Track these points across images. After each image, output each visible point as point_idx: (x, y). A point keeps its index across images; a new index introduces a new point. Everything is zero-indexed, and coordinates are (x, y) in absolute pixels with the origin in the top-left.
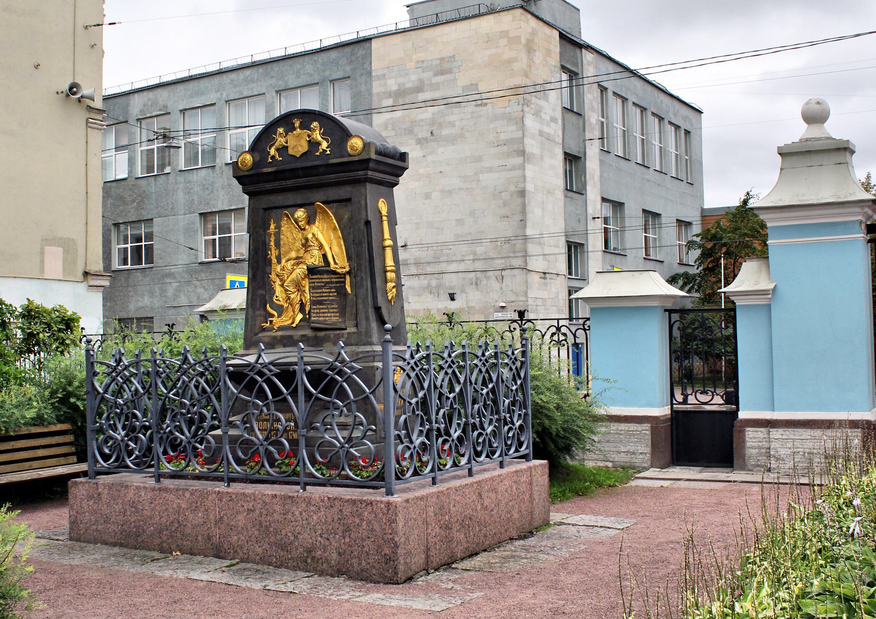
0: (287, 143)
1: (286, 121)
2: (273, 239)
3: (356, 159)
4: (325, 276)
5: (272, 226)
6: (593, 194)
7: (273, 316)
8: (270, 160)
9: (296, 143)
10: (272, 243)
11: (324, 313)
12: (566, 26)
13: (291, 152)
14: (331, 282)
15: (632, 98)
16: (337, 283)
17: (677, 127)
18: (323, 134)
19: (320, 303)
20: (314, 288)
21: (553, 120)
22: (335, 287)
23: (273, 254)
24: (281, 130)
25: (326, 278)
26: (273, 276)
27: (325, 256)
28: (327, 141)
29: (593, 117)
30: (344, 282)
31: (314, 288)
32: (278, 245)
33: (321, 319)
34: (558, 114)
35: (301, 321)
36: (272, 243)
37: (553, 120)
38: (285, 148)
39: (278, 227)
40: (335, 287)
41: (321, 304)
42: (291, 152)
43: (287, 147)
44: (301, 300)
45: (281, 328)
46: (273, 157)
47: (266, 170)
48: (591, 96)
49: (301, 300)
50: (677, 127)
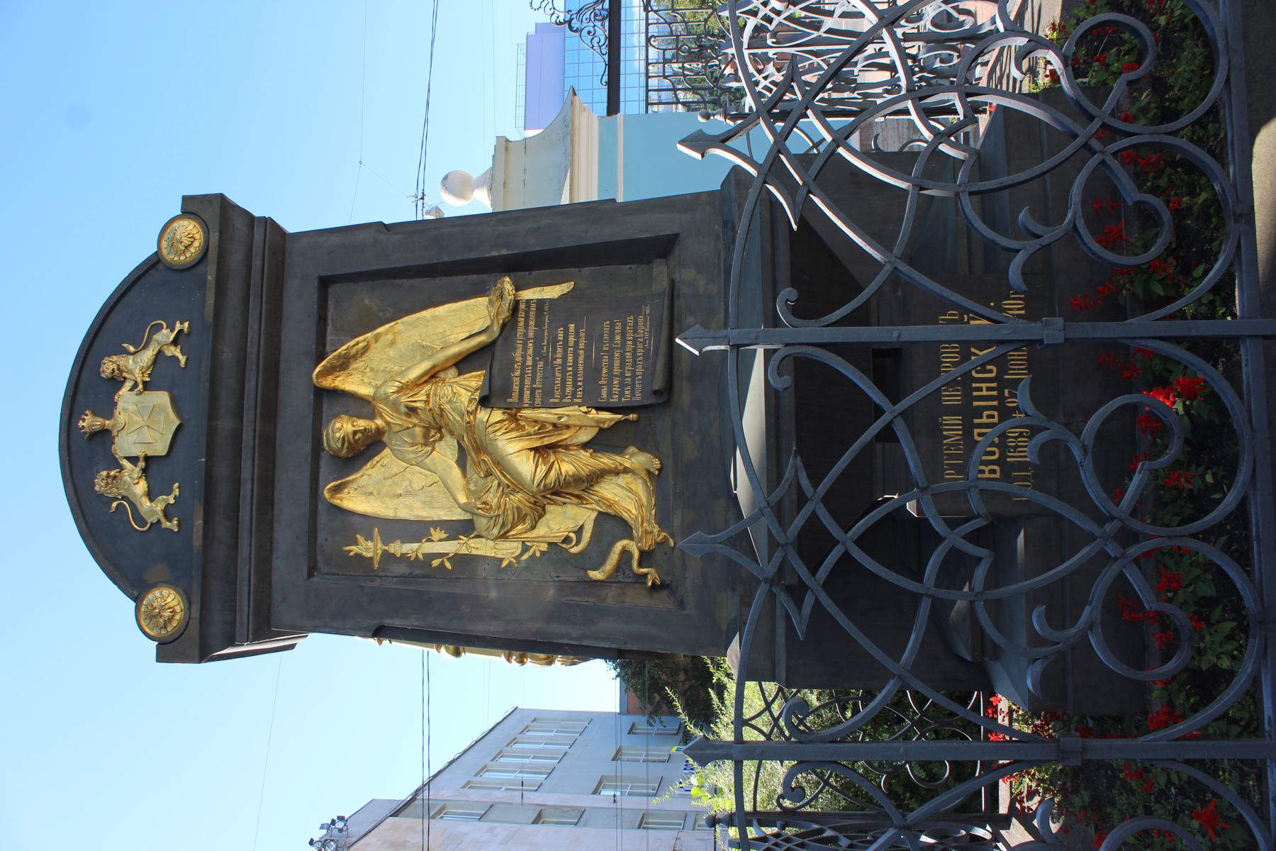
0: (133, 460)
1: (83, 454)
2: (399, 548)
3: (215, 237)
4: (518, 355)
5: (368, 548)
6: (587, 801)
7: (625, 554)
8: (173, 525)
9: (144, 423)
10: (408, 548)
11: (622, 366)
12: (387, 811)
13: (161, 448)
14: (538, 340)
15: (487, 761)
16: (539, 324)
17: (527, 729)
18: (141, 346)
19: (593, 372)
20: (548, 393)
21: (491, 830)
22: (553, 330)
23: (440, 546)
24: (100, 485)
25: (522, 354)
26: (508, 551)
27: (464, 363)
28: (158, 328)
29: (498, 795)
30: (541, 303)
31: (548, 393)
32: (418, 530)
33: (639, 370)
34: (485, 825)
35: (643, 448)
36: (408, 548)
37: (491, 830)
38: (150, 464)
39: (368, 523)
40: (553, 330)
41: (599, 370)
42: (161, 448)
43: (148, 459)
44: (585, 446)
45: (663, 519)
46: (167, 513)
47: (197, 542)
48: (474, 795)
49: (585, 446)
50: (527, 729)
